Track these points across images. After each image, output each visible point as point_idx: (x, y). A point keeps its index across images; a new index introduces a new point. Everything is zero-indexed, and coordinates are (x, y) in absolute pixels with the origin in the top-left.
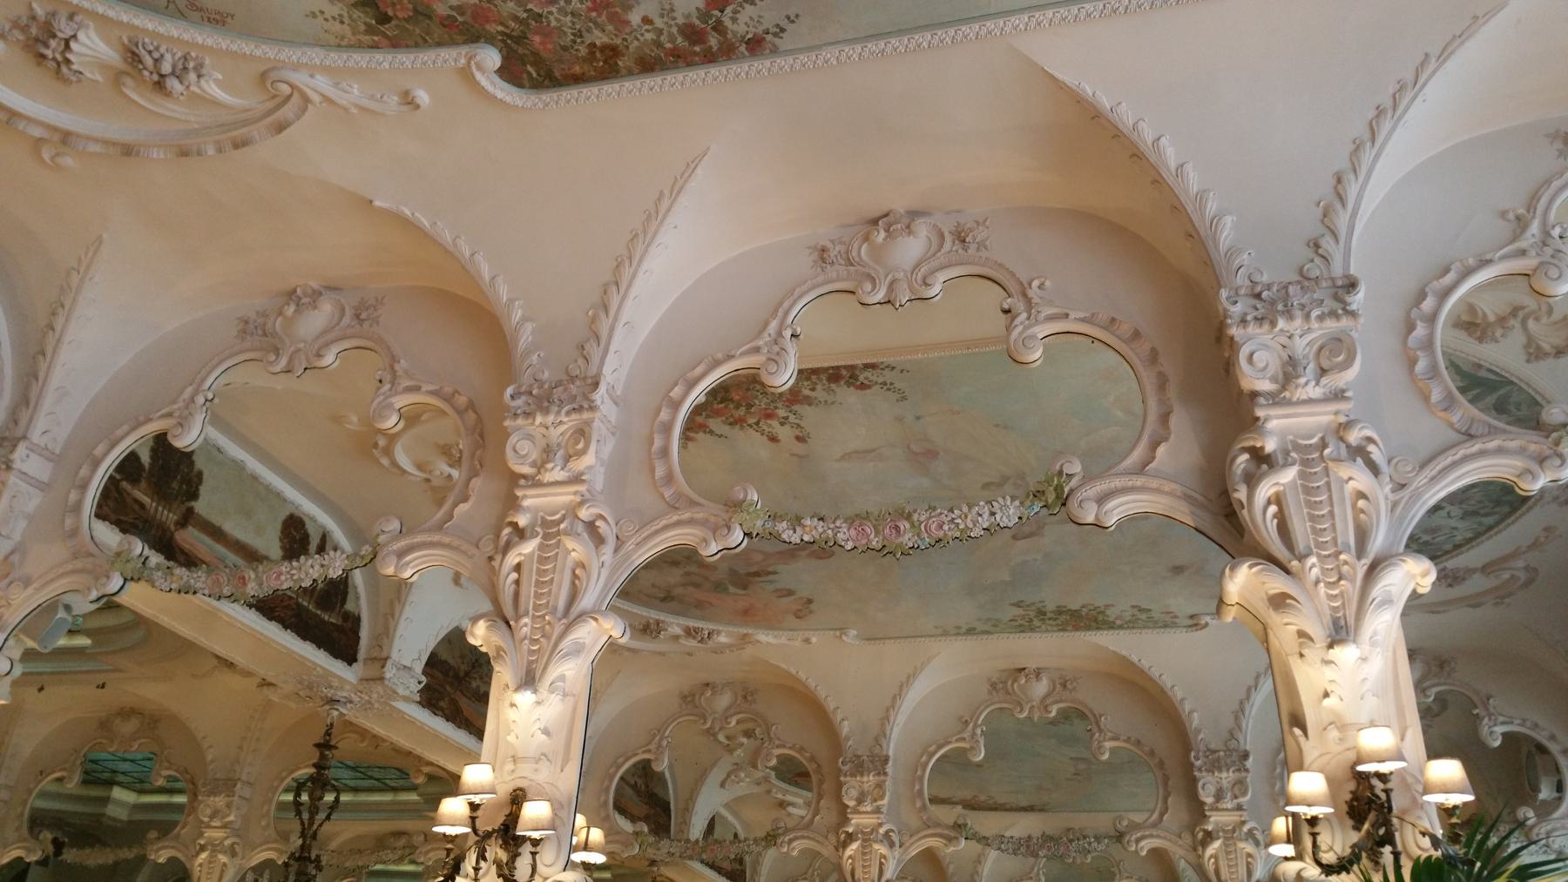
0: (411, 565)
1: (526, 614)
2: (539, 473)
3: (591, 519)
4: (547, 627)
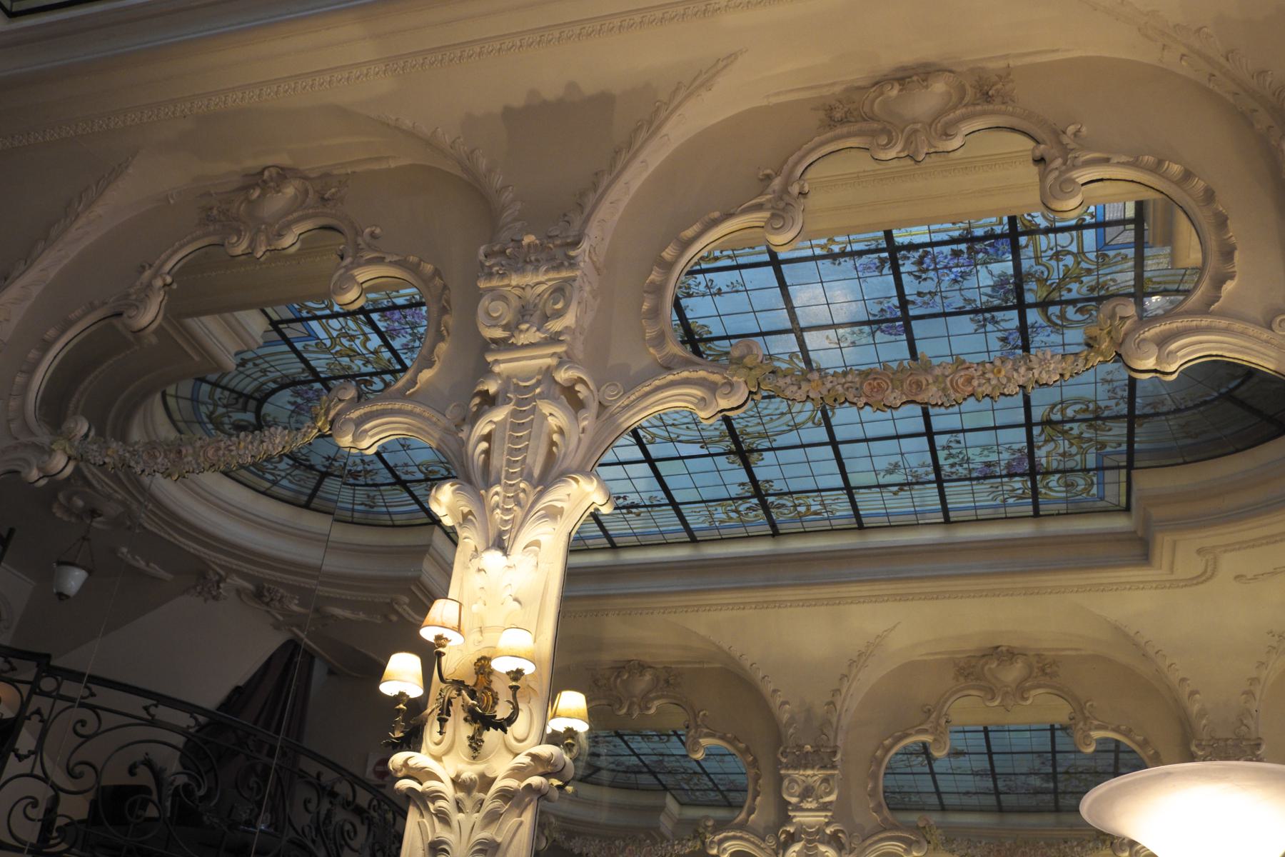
0: (370, 433)
1: (498, 482)
2: (513, 336)
3: (569, 385)
4: (522, 495)
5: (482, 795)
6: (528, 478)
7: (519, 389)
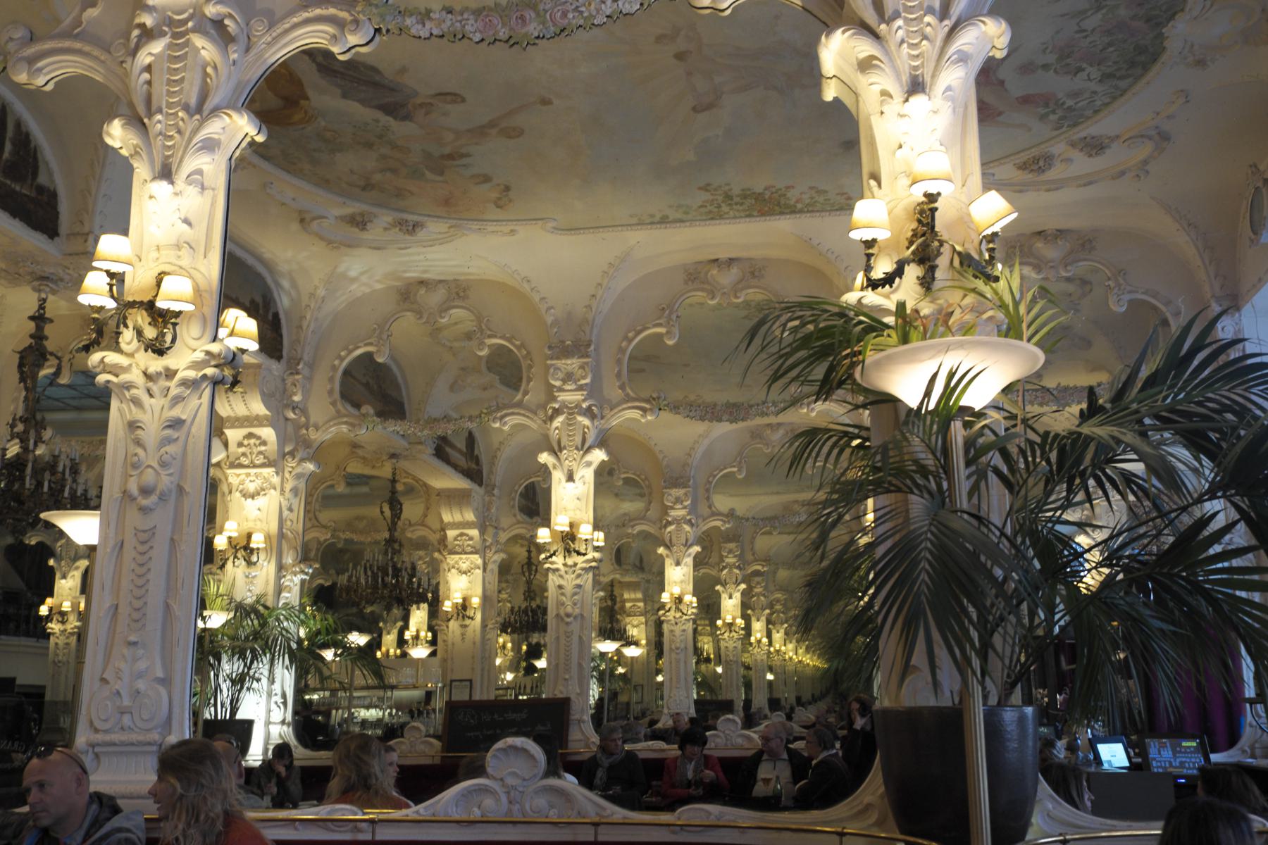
1: (160, 111)
4: (181, 123)
5: (168, 384)
6: (186, 108)
7: (171, 23)
